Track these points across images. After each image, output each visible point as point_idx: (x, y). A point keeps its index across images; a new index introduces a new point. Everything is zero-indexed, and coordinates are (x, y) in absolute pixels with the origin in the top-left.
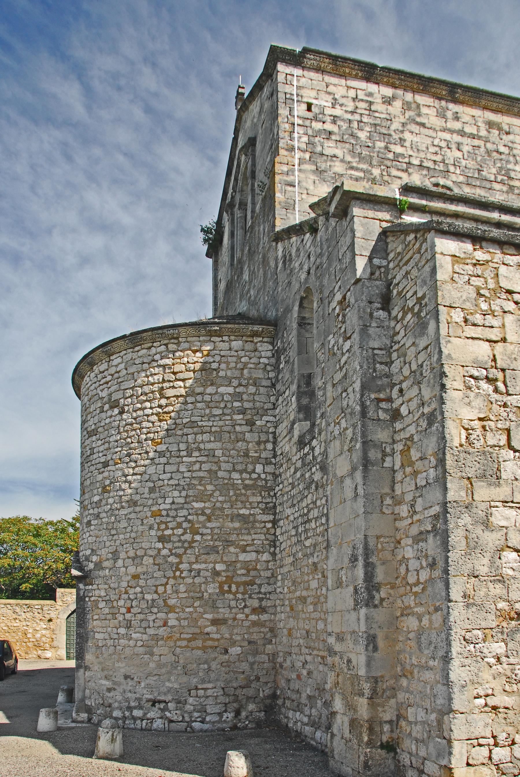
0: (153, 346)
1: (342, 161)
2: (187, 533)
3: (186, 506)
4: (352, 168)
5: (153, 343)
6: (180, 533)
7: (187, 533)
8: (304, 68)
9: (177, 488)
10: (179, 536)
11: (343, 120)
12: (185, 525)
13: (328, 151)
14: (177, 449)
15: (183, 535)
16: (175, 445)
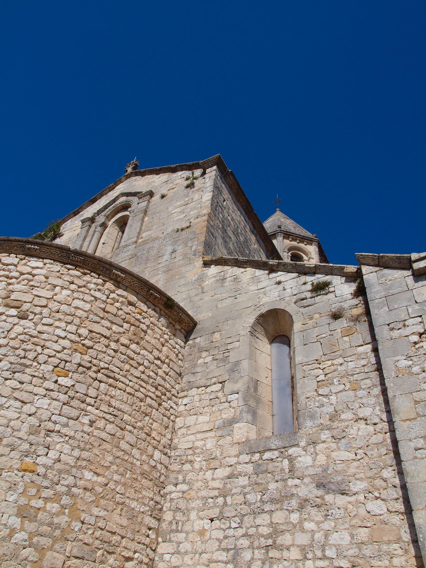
0: (89, 274)
1: (233, 244)
2: (64, 513)
3: (74, 470)
4: (236, 252)
5: (92, 272)
6: (54, 511)
7: (64, 513)
8: (225, 180)
9: (71, 441)
10: (53, 515)
11: (236, 222)
12: (65, 500)
13: (228, 232)
14: (85, 392)
15: (57, 514)
16: (85, 387)
